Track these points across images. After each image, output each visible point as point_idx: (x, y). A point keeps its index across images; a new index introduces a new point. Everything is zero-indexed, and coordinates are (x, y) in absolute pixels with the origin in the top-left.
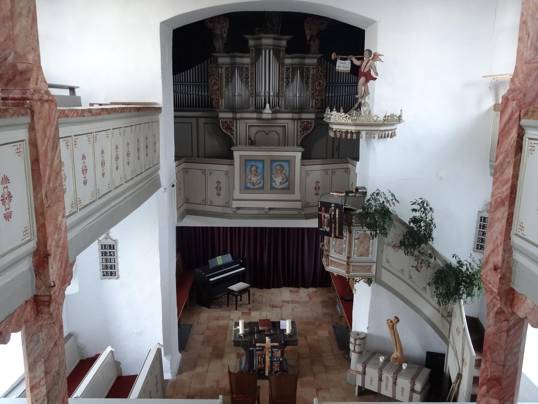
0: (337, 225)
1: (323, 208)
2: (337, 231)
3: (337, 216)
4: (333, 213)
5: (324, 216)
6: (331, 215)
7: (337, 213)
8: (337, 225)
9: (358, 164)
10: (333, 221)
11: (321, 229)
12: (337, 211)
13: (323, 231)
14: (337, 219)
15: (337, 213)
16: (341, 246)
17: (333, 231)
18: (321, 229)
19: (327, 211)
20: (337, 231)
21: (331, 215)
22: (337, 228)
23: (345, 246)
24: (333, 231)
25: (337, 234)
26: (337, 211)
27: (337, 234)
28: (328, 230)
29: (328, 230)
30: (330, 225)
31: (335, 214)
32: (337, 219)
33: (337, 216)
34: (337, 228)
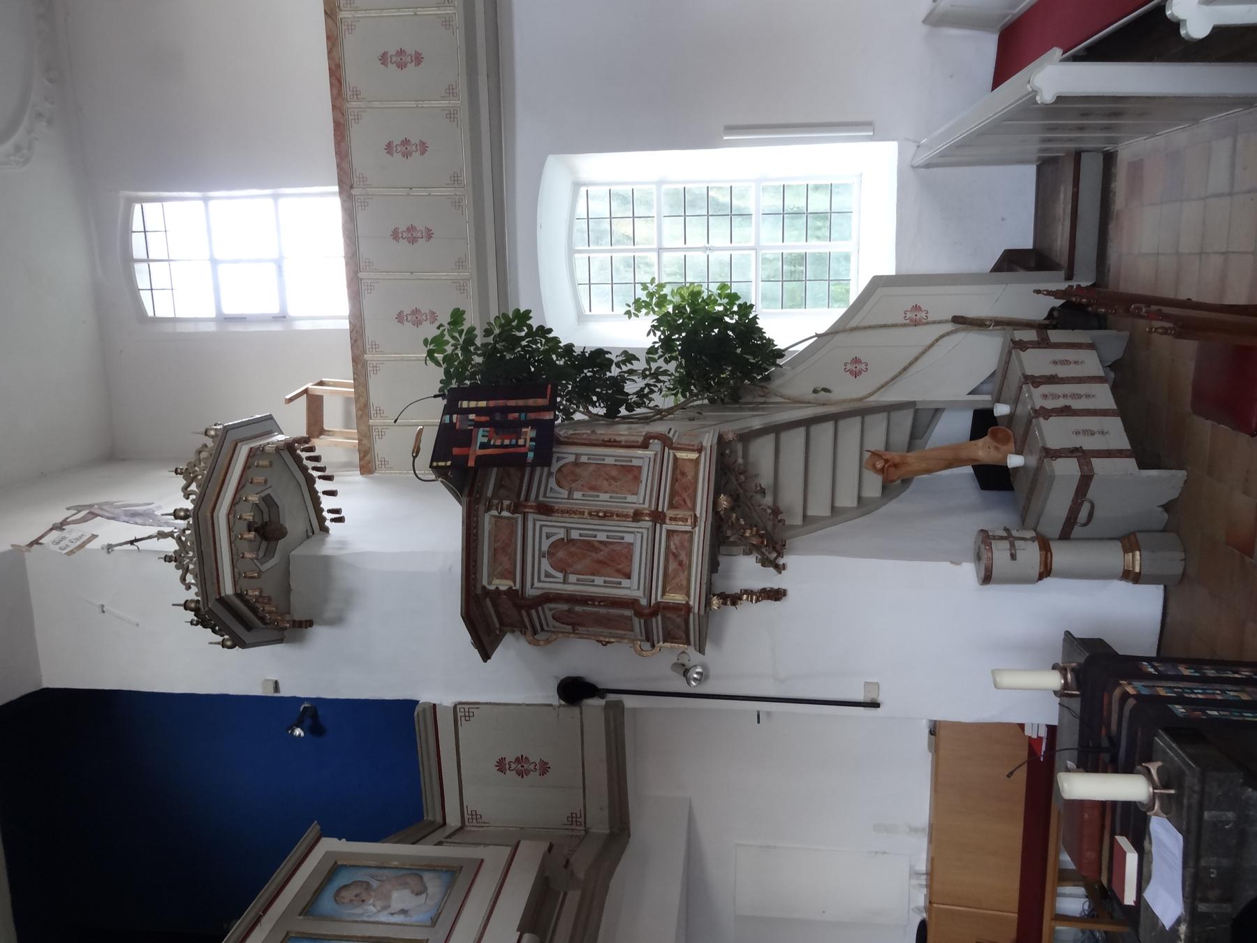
0: (512, 403)
1: (456, 451)
2: (531, 402)
3: (483, 404)
4: (472, 416)
5: (483, 446)
6: (478, 425)
7: (473, 404)
8: (512, 403)
9: (425, 696)
10: (498, 417)
11: (531, 455)
12: (465, 404)
13: (535, 450)
14: (492, 403)
15: (473, 404)
16: (614, 473)
17: (532, 416)
18: (531, 455)
19: (466, 438)
20: (531, 402)
21: (478, 425)
22: (521, 403)
23: (610, 456)
24: (532, 416)
25: (541, 402)
26: (465, 404)
27: (541, 402)
28: (530, 433)
29: (530, 433)
30: (514, 428)
31: (477, 411)
32: (492, 403)
33: (483, 404)
34: (521, 403)
